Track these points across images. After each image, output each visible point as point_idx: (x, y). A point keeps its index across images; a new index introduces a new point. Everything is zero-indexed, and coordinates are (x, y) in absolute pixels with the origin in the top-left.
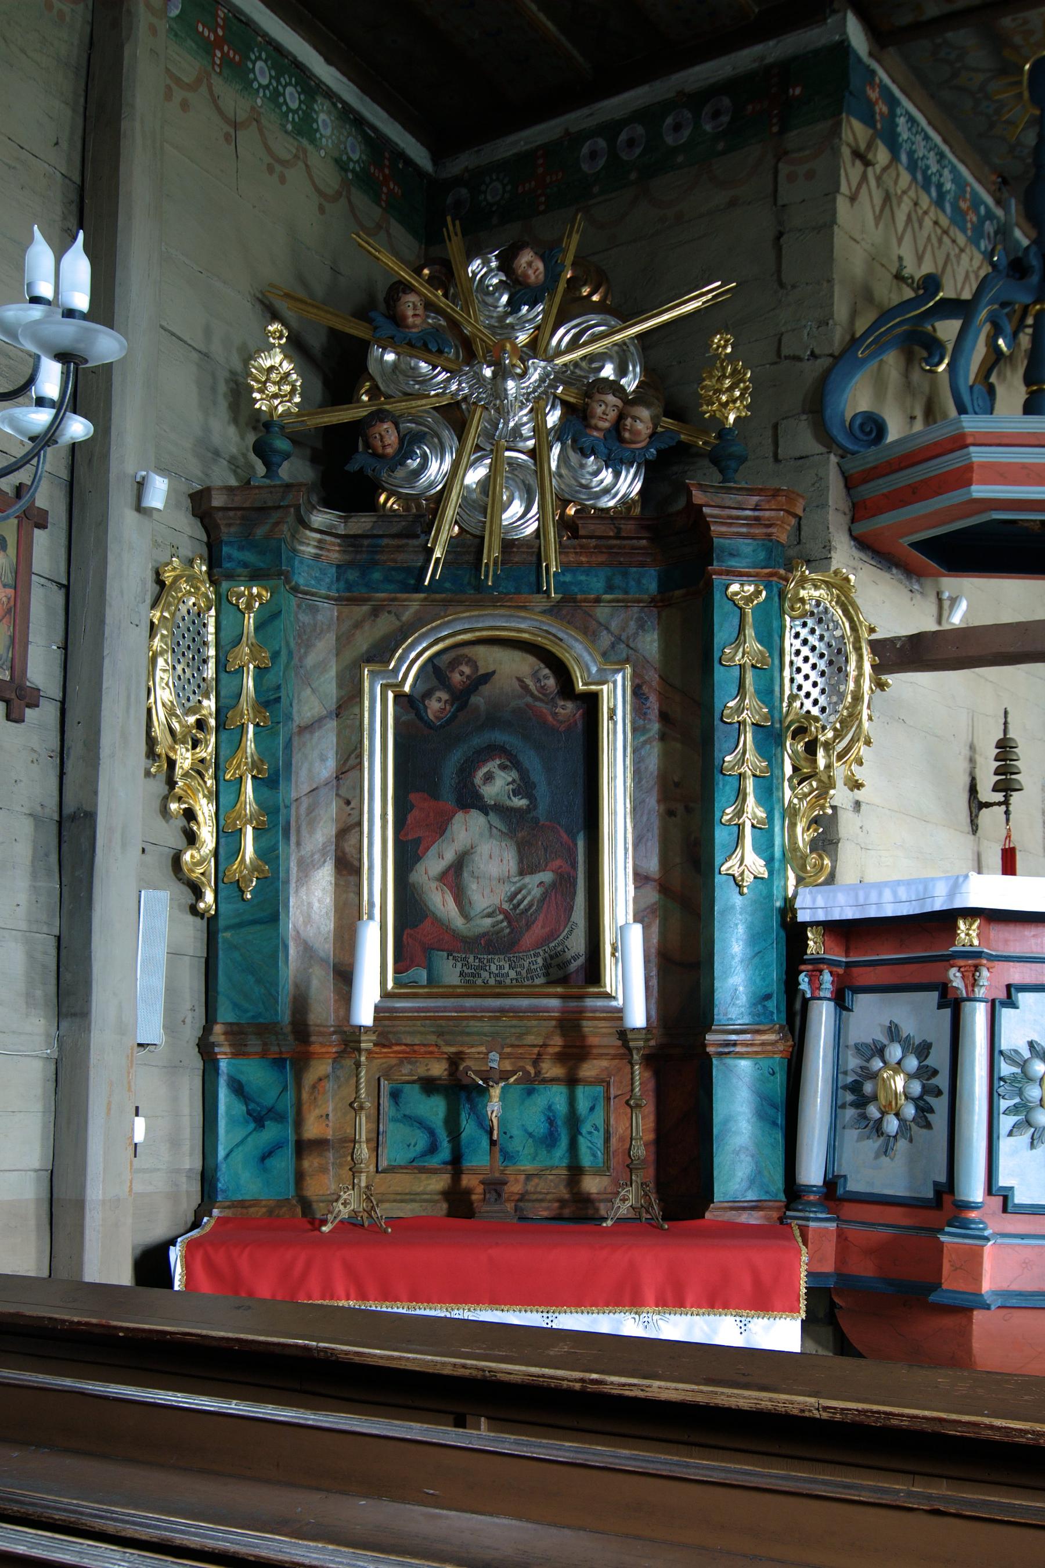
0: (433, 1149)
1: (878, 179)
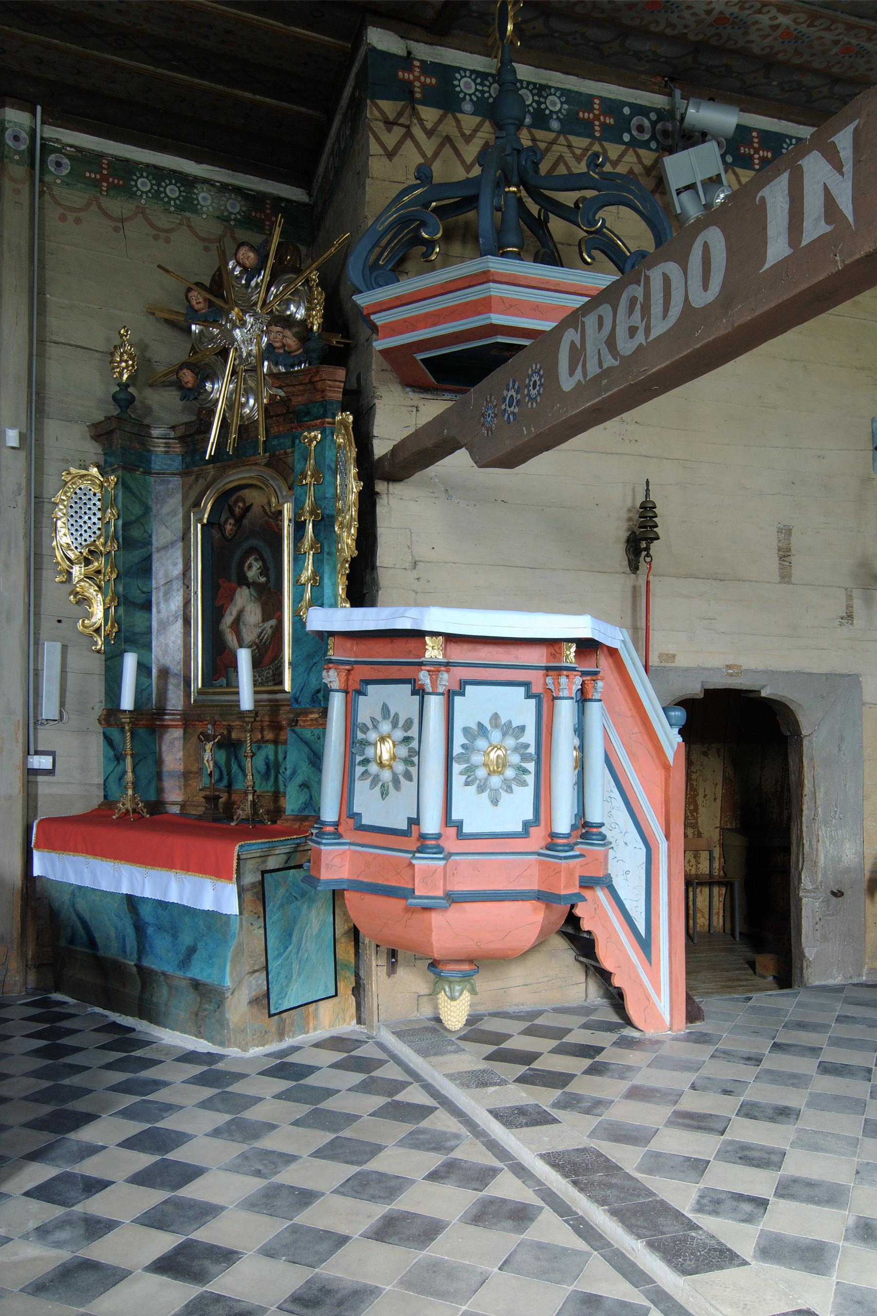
0: (221, 779)
1: (429, 133)
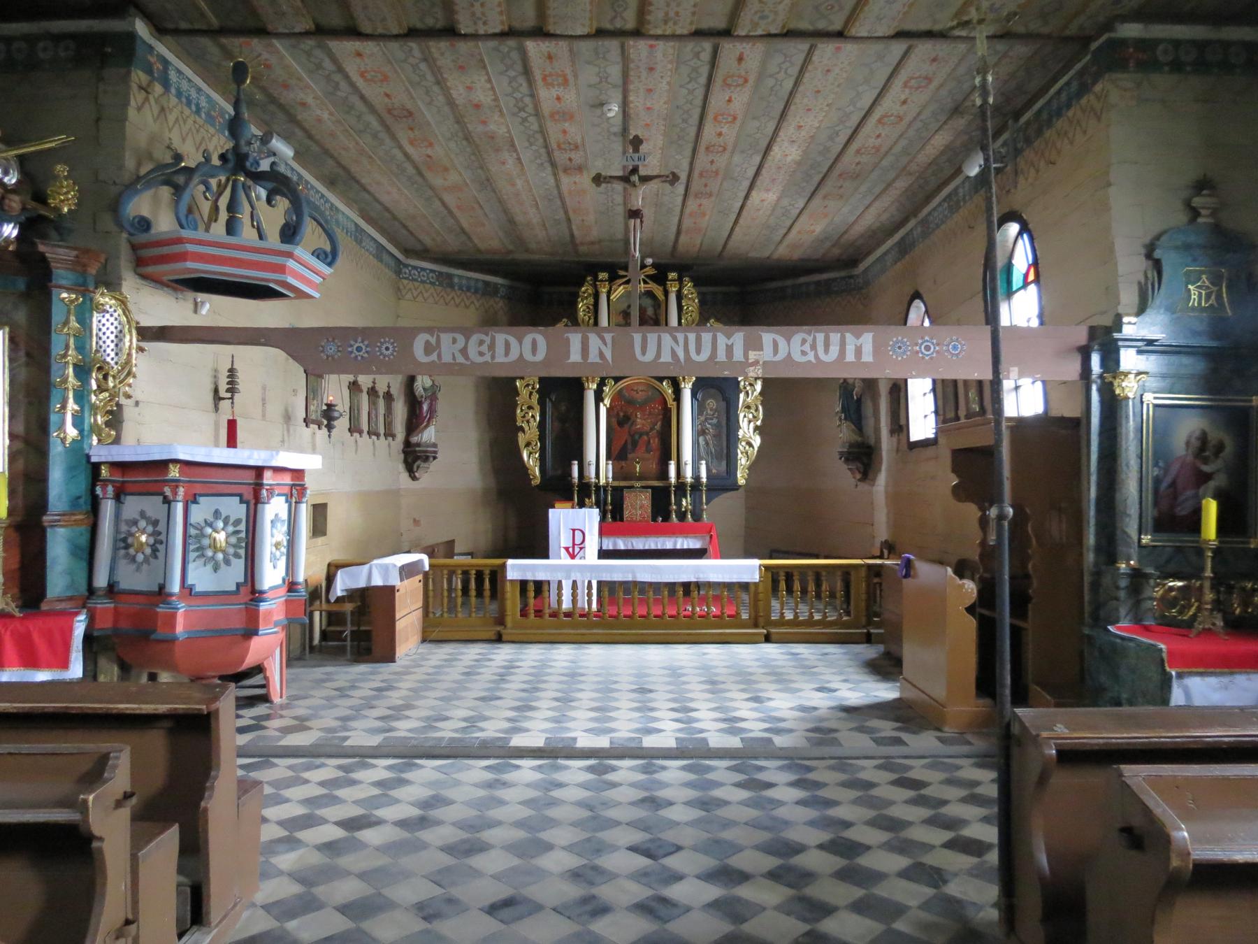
1: (157, 101)
